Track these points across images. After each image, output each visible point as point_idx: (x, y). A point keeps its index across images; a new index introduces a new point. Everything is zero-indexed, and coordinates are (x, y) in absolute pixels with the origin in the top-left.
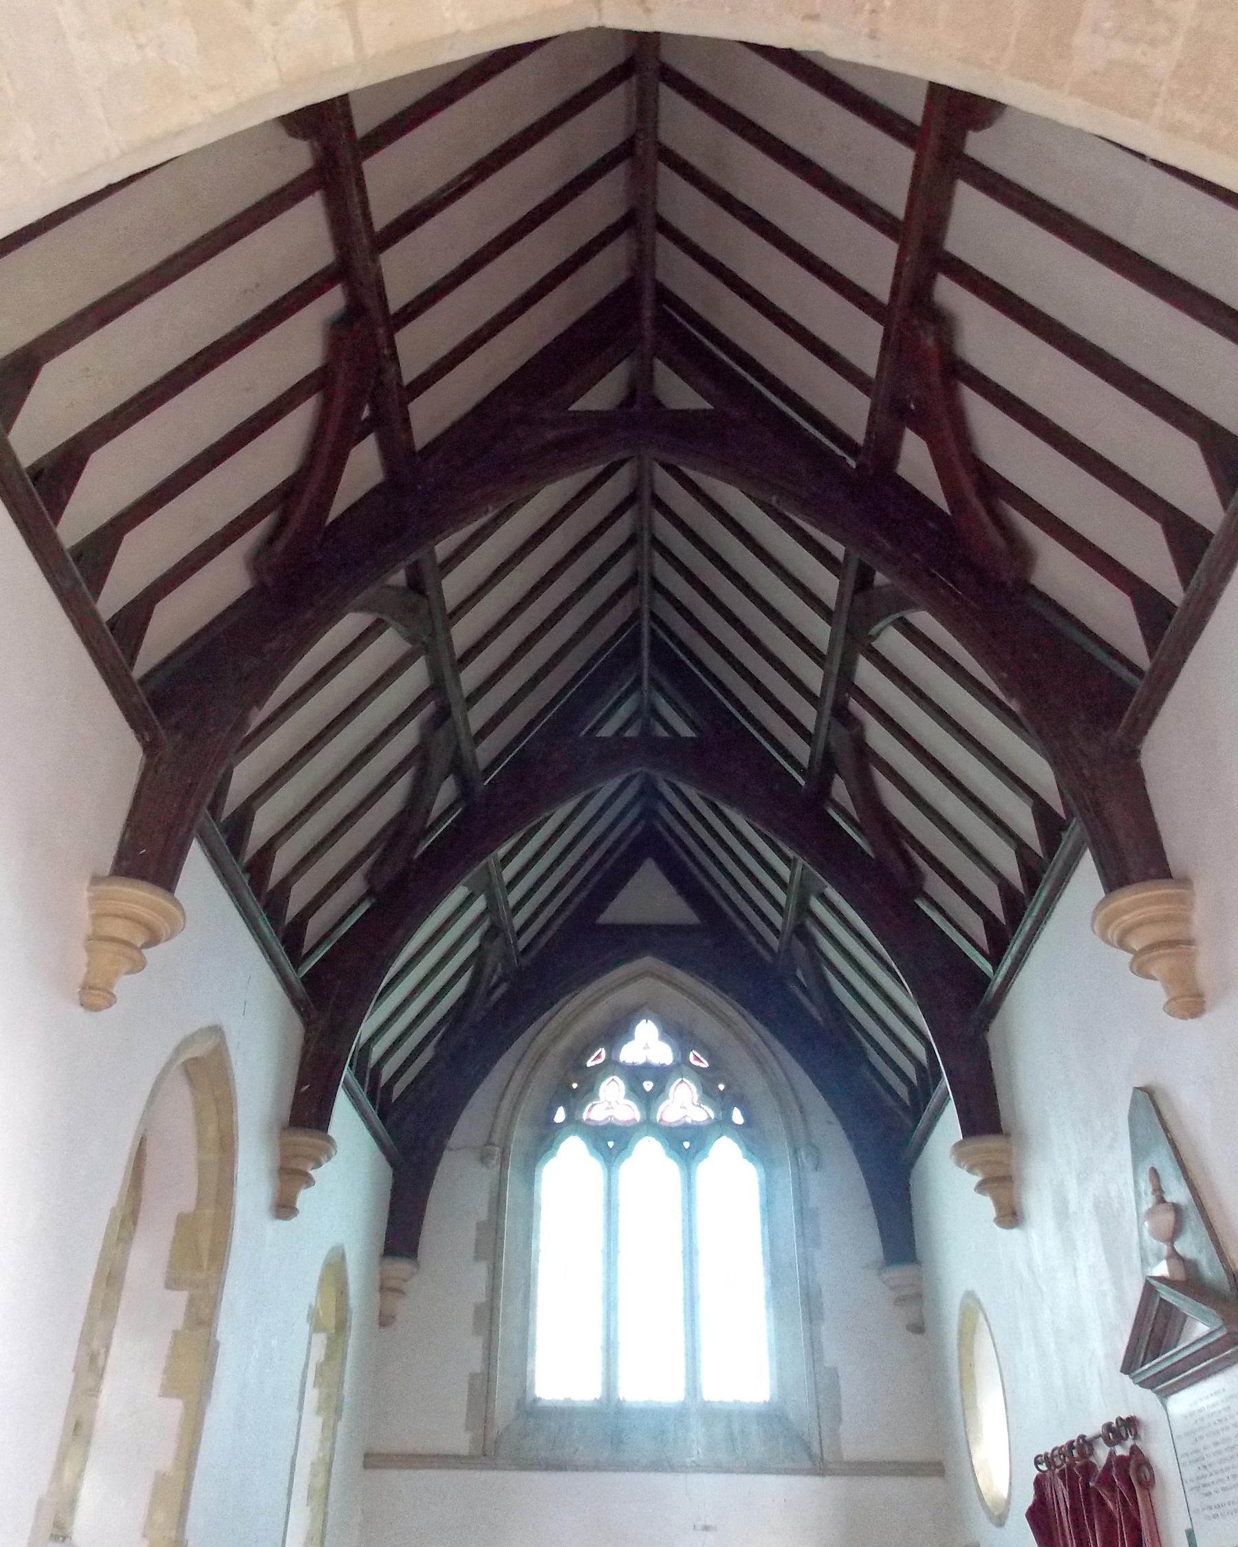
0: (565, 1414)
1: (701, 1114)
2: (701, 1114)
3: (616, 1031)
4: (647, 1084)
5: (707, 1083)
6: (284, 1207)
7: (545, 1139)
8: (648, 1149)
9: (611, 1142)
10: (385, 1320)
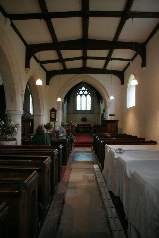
0: (78, 111)
1: (87, 93)
2: (87, 93)
3: (82, 88)
4: (83, 91)
5: (87, 91)
6: (65, 103)
7: (77, 95)
8: (83, 95)
9: (81, 95)
10: (68, 106)
